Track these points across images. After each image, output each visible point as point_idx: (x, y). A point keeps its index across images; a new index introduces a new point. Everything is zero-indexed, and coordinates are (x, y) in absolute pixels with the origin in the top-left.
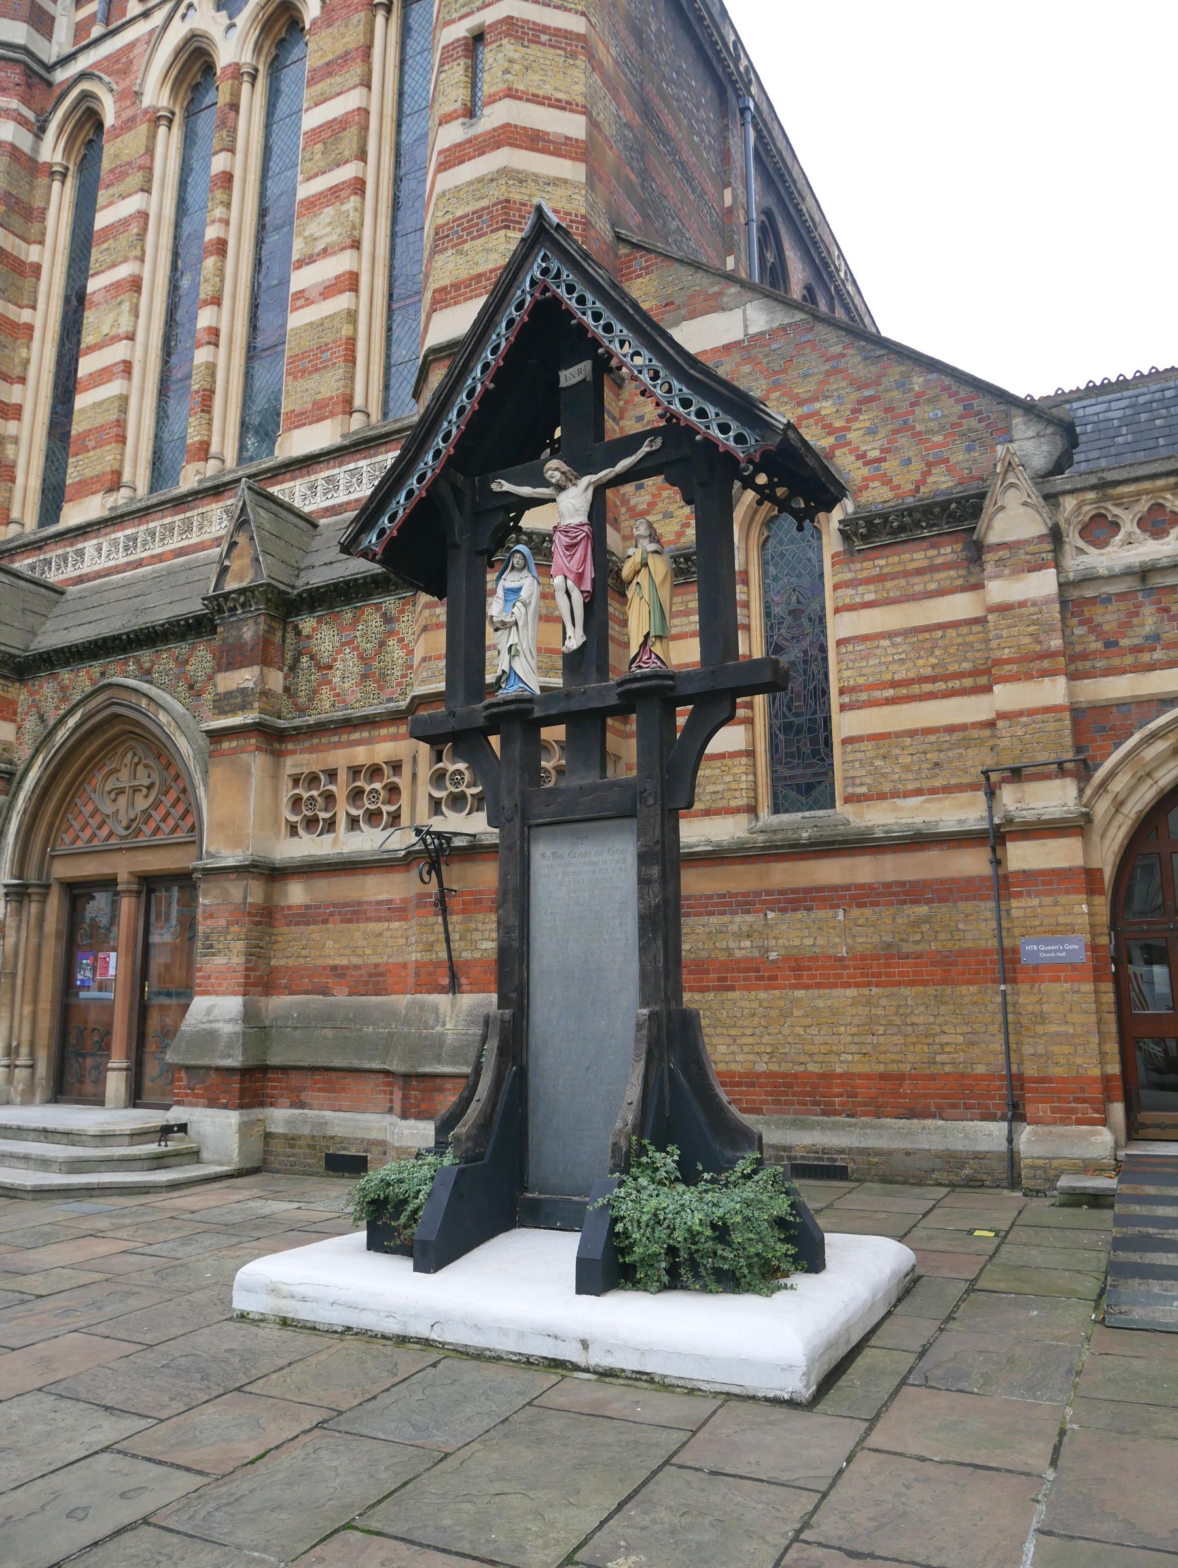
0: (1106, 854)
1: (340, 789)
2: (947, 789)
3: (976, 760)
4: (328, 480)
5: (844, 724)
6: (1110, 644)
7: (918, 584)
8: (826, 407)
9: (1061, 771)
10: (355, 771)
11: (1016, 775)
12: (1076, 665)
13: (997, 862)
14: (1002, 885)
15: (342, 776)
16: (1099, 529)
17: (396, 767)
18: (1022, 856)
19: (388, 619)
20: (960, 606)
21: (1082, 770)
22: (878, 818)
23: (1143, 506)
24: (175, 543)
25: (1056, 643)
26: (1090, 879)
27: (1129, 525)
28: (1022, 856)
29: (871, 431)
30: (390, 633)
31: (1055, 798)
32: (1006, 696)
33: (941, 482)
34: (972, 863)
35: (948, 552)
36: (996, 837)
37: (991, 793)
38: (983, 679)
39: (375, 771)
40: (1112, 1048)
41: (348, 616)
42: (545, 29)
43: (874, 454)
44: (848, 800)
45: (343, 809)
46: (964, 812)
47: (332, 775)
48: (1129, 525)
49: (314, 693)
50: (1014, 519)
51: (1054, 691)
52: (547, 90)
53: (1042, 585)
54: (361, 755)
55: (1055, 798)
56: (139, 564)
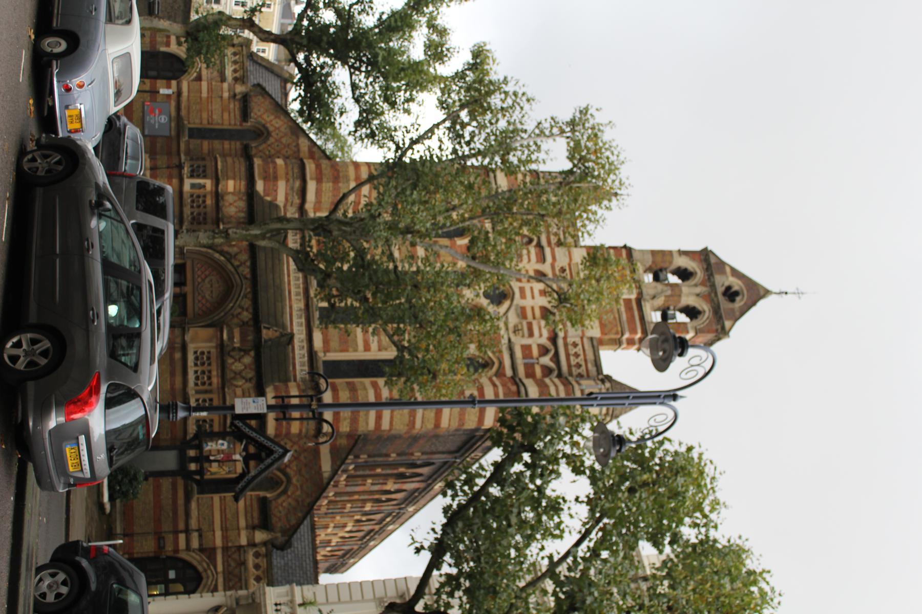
0: (183, 555)
1: (206, 368)
2: (199, 521)
3: (205, 527)
4: (303, 347)
5: (216, 498)
6: (229, 557)
7: (249, 515)
8: (298, 493)
9: (201, 545)
10: (210, 372)
11: (200, 536)
12: (225, 549)
13: (181, 532)
14: (176, 532)
15: (209, 368)
16: (257, 555)
17: (210, 384)
18: (182, 537)
19: (250, 379)
20: (242, 523)
21: (202, 550)
22: (194, 505)
23: (261, 564)
24: (293, 290)
25: (230, 544)
26: (176, 550)
27: (257, 561)
28: (182, 537)
29: (290, 504)
30: (246, 381)
31: (195, 544)
32: (218, 534)
33: (274, 520)
34: (181, 526)
35: (256, 522)
36: (187, 531)
37: (197, 530)
38: (224, 529)
39: (209, 378)
40: (139, 555)
41: (253, 367)
42: (414, 418)
43: (284, 504)
44: (198, 499)
45: (200, 369)
46: (193, 523)
47: (209, 364)
48: (257, 561)
49: (232, 357)
50: (260, 536)
51: (219, 542)
52: (395, 419)
53: (244, 541)
54: (214, 373)
55: (195, 544)
56: (289, 276)
